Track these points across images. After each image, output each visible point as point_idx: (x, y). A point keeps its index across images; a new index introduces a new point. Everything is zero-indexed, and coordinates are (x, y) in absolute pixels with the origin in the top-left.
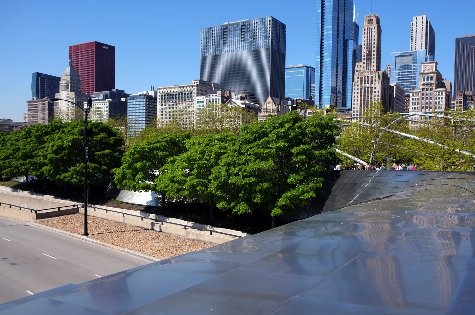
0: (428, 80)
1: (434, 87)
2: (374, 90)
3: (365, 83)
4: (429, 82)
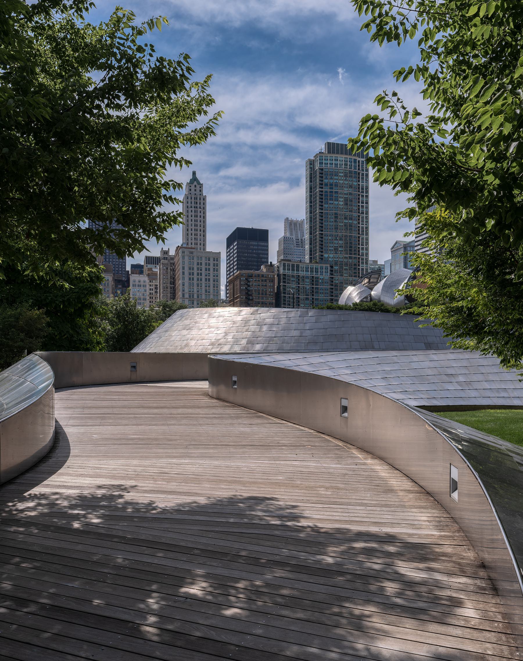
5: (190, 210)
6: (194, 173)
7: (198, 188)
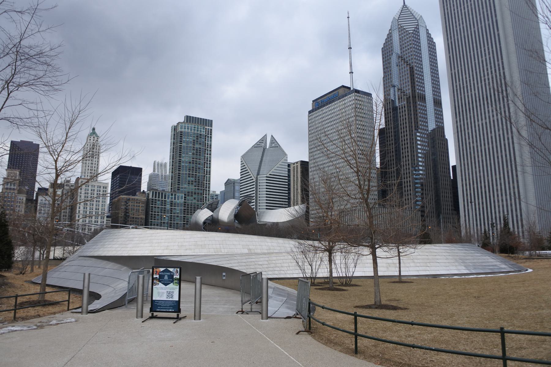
7: (96, 139)
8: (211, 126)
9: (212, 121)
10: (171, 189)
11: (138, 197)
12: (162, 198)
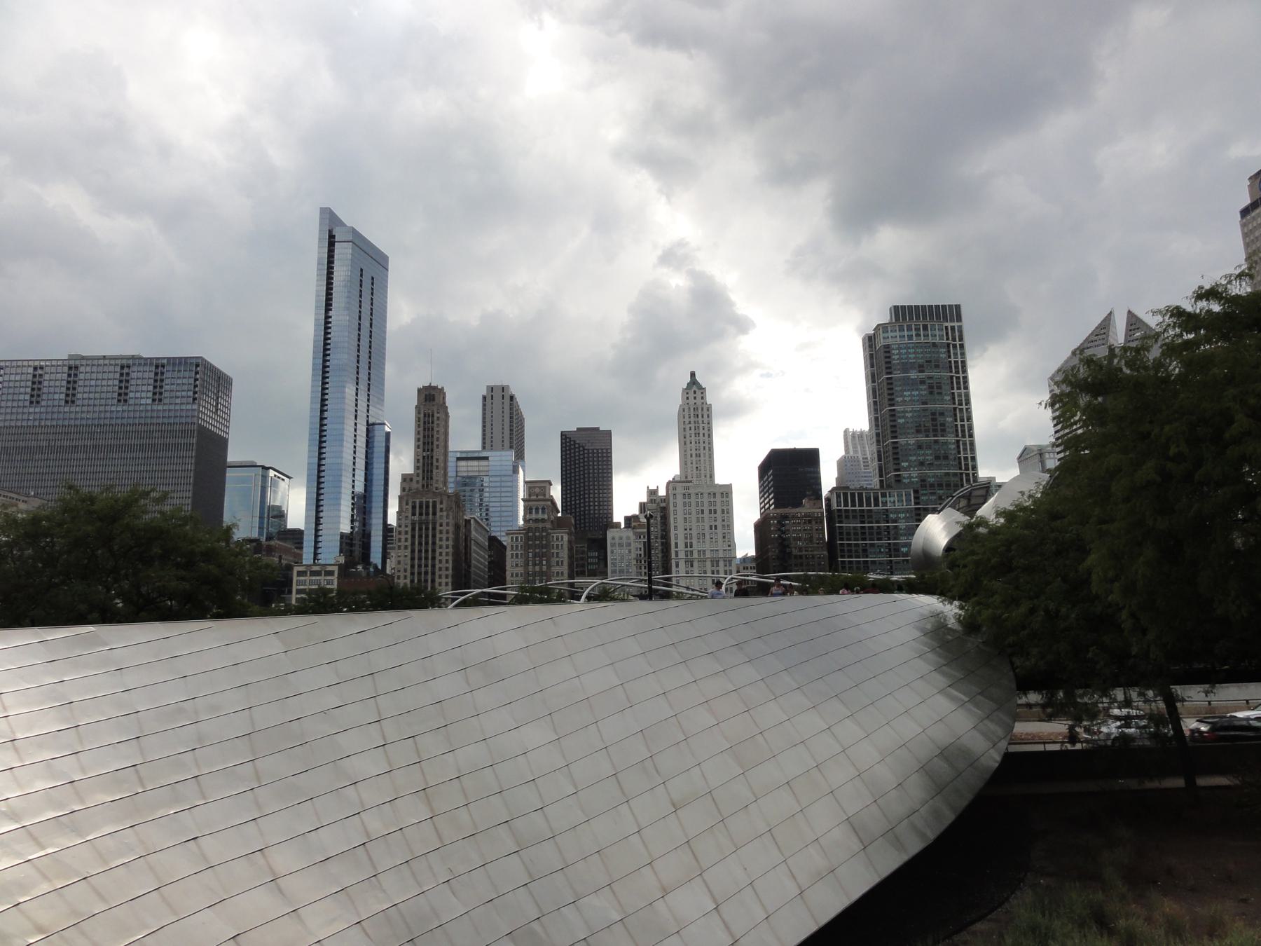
0: (537, 512)
1: (548, 525)
2: (438, 528)
3: (421, 514)
4: (540, 516)
5: (688, 427)
6: (693, 374)
7: (699, 393)
8: (959, 319)
9: (958, 307)
10: (881, 482)
11: (807, 507)
12: (861, 504)
